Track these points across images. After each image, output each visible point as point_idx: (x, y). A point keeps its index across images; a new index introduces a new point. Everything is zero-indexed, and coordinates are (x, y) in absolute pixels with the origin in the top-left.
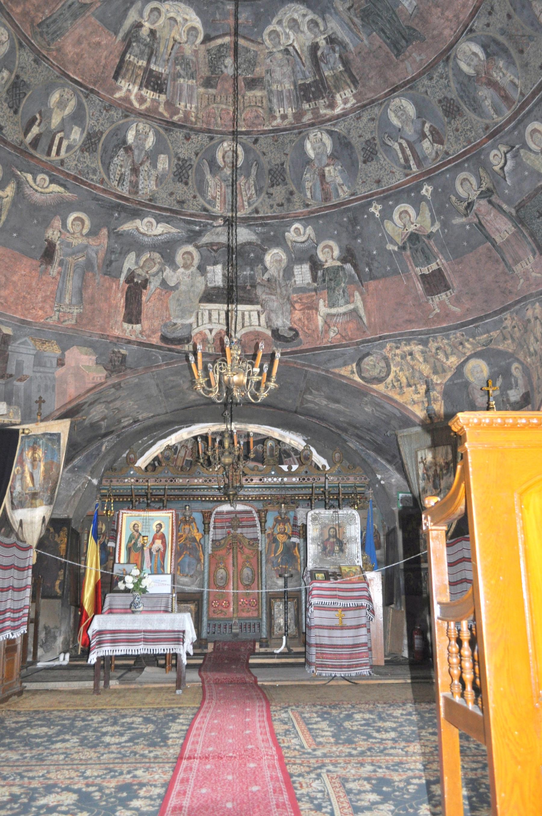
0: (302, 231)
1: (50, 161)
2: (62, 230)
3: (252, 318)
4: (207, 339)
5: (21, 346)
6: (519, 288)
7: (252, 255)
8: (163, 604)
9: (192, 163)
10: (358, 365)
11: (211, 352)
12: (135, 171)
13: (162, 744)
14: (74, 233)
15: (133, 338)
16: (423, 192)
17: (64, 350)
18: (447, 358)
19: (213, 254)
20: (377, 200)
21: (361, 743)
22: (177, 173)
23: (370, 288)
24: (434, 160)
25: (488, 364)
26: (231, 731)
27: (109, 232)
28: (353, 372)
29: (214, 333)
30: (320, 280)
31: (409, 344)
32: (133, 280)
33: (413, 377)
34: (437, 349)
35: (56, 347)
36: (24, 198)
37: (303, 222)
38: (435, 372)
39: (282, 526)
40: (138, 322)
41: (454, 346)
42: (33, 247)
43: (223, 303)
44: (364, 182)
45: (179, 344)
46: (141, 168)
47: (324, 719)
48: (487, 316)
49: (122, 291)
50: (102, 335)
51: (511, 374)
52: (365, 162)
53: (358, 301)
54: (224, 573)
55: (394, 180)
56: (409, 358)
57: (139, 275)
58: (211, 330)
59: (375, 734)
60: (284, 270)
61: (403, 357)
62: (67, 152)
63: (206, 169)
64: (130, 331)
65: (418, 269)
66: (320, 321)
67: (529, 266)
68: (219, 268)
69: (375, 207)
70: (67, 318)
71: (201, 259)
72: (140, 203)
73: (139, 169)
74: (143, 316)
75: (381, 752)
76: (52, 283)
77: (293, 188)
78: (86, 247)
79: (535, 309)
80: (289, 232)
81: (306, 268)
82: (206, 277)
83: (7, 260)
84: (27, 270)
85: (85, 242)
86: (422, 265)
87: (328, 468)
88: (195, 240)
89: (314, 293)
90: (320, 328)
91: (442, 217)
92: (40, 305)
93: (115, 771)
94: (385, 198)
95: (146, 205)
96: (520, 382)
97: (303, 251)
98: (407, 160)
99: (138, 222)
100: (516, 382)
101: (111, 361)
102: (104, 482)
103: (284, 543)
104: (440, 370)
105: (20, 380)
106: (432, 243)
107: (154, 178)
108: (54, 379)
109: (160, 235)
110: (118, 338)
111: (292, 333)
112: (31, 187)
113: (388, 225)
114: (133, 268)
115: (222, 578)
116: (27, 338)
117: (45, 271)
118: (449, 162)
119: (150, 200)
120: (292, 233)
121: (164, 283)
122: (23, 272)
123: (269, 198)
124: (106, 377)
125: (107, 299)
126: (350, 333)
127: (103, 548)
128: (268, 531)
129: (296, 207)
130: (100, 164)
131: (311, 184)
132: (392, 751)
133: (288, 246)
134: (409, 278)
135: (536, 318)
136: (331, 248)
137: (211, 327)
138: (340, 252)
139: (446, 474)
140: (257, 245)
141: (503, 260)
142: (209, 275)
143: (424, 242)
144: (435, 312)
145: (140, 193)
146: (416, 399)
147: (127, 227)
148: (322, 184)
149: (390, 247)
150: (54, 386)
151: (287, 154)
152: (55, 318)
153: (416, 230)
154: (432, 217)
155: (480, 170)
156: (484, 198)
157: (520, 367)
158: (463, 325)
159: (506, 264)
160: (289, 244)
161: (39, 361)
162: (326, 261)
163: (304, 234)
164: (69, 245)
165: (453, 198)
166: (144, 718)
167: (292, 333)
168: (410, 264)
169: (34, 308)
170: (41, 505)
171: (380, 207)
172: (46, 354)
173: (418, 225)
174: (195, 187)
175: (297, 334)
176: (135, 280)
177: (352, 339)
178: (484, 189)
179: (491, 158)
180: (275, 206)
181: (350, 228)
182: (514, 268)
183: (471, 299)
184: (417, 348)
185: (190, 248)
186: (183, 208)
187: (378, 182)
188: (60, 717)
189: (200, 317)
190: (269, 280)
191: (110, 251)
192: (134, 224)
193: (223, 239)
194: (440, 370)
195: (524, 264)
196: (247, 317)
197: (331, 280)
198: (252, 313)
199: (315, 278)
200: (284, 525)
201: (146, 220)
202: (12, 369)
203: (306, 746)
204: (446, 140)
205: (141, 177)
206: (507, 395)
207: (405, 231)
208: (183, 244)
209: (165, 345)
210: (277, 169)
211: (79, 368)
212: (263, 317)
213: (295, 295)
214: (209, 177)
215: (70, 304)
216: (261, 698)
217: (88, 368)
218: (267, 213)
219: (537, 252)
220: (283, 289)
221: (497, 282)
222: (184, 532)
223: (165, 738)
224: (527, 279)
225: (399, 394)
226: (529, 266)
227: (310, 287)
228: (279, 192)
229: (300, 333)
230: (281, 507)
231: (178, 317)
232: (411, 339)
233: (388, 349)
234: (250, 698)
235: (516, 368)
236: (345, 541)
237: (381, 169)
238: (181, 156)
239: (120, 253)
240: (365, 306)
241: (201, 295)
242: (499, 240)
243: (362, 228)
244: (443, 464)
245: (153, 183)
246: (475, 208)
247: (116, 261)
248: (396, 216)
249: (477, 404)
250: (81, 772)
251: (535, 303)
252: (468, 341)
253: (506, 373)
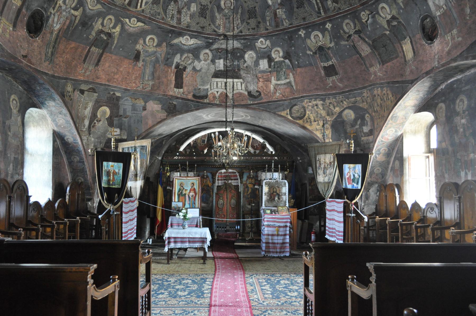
0: (264, 43)
1: (137, 11)
2: (144, 45)
3: (238, 86)
4: (216, 96)
5: (126, 101)
6: (371, 79)
7: (238, 54)
8: (196, 222)
9: (208, 7)
10: (290, 110)
11: (217, 103)
12: (179, 12)
13: (202, 297)
14: (149, 46)
15: (179, 96)
16: (327, 26)
17: (146, 102)
18: (335, 108)
19: (219, 54)
20: (303, 28)
21: (282, 298)
22: (200, 12)
23: (298, 72)
24: (333, 11)
25: (354, 113)
26: (229, 289)
27: (166, 44)
28: (287, 114)
29: (219, 93)
30: (273, 67)
31: (316, 101)
32: (179, 67)
33: (317, 117)
34: (330, 103)
35: (142, 101)
36: (125, 31)
37: (265, 38)
38: (328, 115)
39: (250, 180)
40: (181, 87)
41: (338, 103)
42: (130, 54)
43: (224, 78)
44: (296, 18)
45: (202, 99)
46: (182, 11)
47: (268, 283)
48: (355, 90)
49: (174, 72)
50: (164, 94)
51: (365, 119)
52: (297, 8)
53: (291, 78)
54: (223, 202)
55: (312, 19)
56: (315, 107)
57: (181, 65)
58: (217, 92)
59: (289, 294)
60: (255, 62)
61: (313, 107)
62: (145, 5)
63: (216, 10)
64: (178, 92)
65: (322, 64)
66: (272, 87)
67: (377, 70)
68: (222, 61)
69: (302, 32)
70: (146, 87)
71: (213, 57)
72: (182, 29)
73: (181, 10)
74: (184, 85)
75: (290, 304)
76: (139, 70)
77: (260, 19)
78: (156, 52)
79: (378, 91)
80: (258, 43)
81: (266, 61)
82: (215, 65)
83: (117, 61)
84: (127, 65)
85: (155, 50)
86: (325, 62)
87: (274, 153)
88: (210, 47)
89: (269, 74)
90: (272, 91)
91: (336, 40)
92: (134, 81)
93: (186, 311)
94: (308, 27)
95: (185, 30)
96: (369, 123)
97: (265, 53)
98: (319, 9)
99: (181, 39)
100: (367, 123)
101: (169, 108)
102: (164, 158)
103: (251, 188)
104: (330, 113)
105: (125, 118)
106: (330, 52)
107: (189, 16)
108: (142, 117)
109: (192, 45)
110: (172, 96)
111: (258, 94)
112: (128, 25)
113: (308, 41)
114: (179, 61)
115: (221, 204)
116: (127, 98)
117: (136, 65)
118: (341, 13)
119: (187, 27)
120: (259, 43)
121: (194, 68)
122: (125, 66)
123: (248, 25)
124: (167, 116)
125: (166, 77)
126: (286, 94)
127: (165, 190)
128: (244, 182)
129: (261, 30)
130: (162, 10)
131: (269, 18)
132: (294, 303)
133: (256, 49)
134: (317, 68)
135: (378, 95)
136: (278, 51)
137: (217, 90)
138: (283, 53)
139: (330, 168)
140: (241, 49)
141: (365, 64)
142: (217, 64)
143: (326, 51)
144: (330, 85)
145: (182, 23)
146: (318, 128)
147: (176, 41)
148: (275, 18)
149: (309, 52)
150: (142, 121)
151: (257, 2)
152: (141, 87)
153: (322, 45)
154: (330, 39)
155: (356, 20)
156: (357, 34)
157: (369, 116)
158: (343, 92)
159: (366, 66)
160: (258, 49)
161: (134, 108)
162: (276, 58)
163: (265, 44)
164: (147, 51)
165: (342, 32)
166: (192, 280)
167: (258, 94)
168: (318, 61)
169: (131, 83)
170: (139, 180)
171: (304, 32)
172: (137, 105)
173: (323, 43)
174: (210, 19)
175: (260, 94)
176: (180, 67)
177: (287, 97)
178: (357, 30)
179: (361, 15)
180: (251, 30)
181: (289, 42)
182: (370, 69)
183: (348, 81)
184: (320, 103)
185: (207, 51)
186: (203, 31)
187: (304, 19)
188: (156, 279)
189: (212, 85)
190: (247, 67)
191: (168, 53)
192: (179, 40)
193: (224, 46)
194: (330, 113)
195: (374, 68)
196: (235, 85)
197: (278, 67)
198: (238, 83)
199: (270, 66)
200: (252, 179)
201: (185, 37)
202: (121, 112)
203: (260, 300)
204: (339, 3)
205: (182, 15)
206: (362, 128)
207: (316, 45)
208: (204, 49)
209: (195, 100)
210: (252, 10)
211: (153, 111)
212: (243, 85)
213: (260, 74)
214: (217, 14)
215: (148, 80)
216: (241, 269)
217: (158, 111)
218: (246, 33)
219: (381, 63)
220: (254, 71)
221: (361, 74)
223: (203, 293)
224: (376, 75)
225: (310, 125)
226: (377, 70)
227: (268, 71)
228: (253, 22)
229: (262, 93)
230: (250, 172)
231: (201, 85)
232: (317, 98)
233: (306, 103)
234: (236, 269)
235: (368, 116)
236: (280, 194)
237: (306, 12)
238: (203, 4)
239: (172, 54)
240: (295, 81)
241: (212, 74)
242: (363, 54)
243: (295, 42)
244: (329, 163)
245: (188, 18)
246: (352, 38)
247: (171, 58)
248: (312, 37)
249: (348, 131)
250: (173, 311)
251: (378, 88)
252: (345, 100)
253: (363, 118)
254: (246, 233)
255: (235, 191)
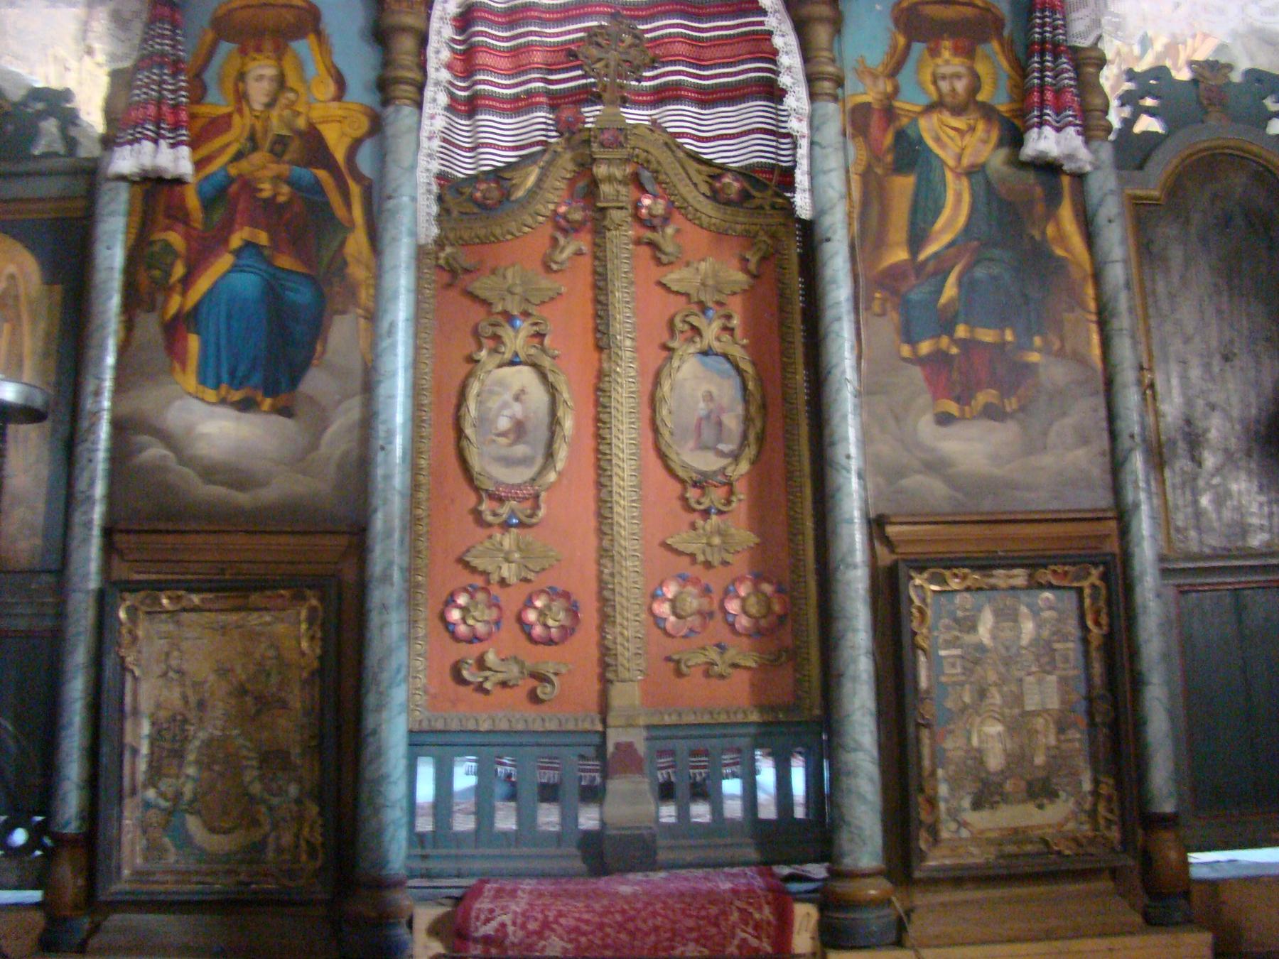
54: (538, 396)
103: (974, 172)
115: (519, 430)
222: (242, 97)
254: (936, 881)
255: (720, 234)
